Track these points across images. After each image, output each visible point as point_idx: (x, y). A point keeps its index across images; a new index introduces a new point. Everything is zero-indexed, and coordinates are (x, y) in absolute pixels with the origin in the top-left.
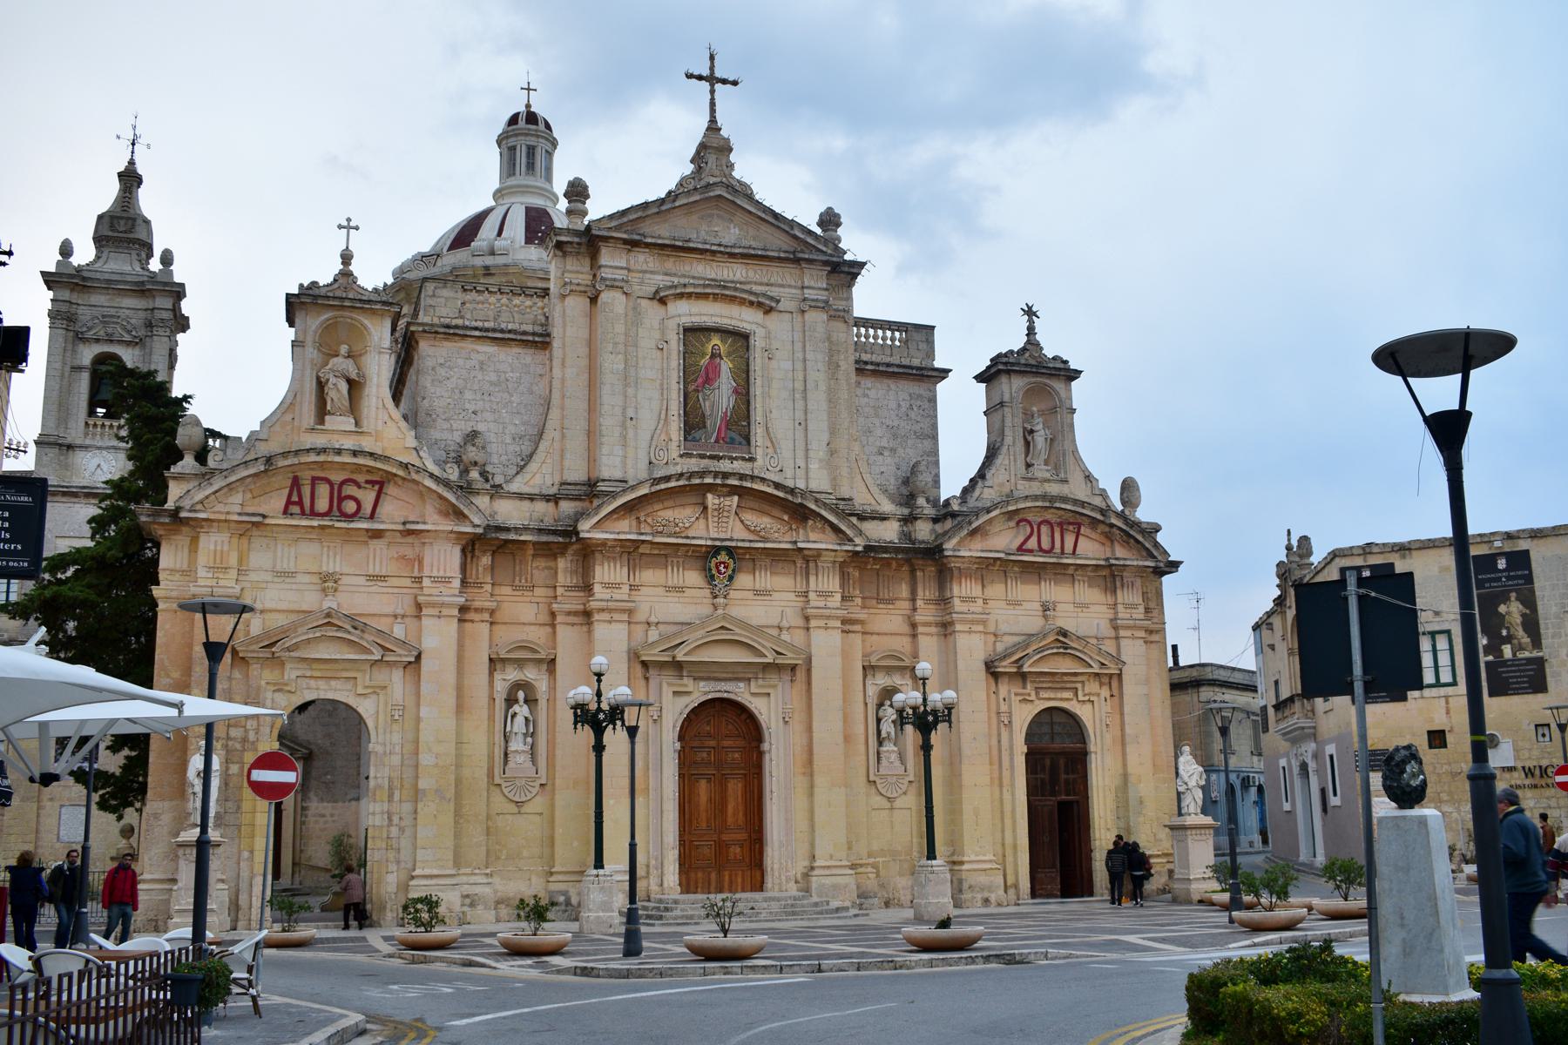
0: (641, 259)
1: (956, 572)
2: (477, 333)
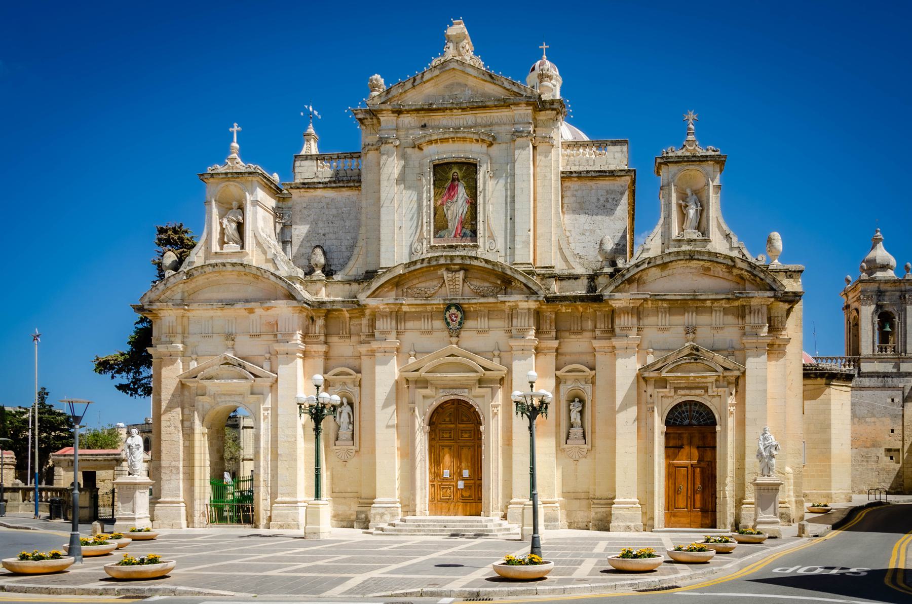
0: (407, 120)
1: (617, 311)
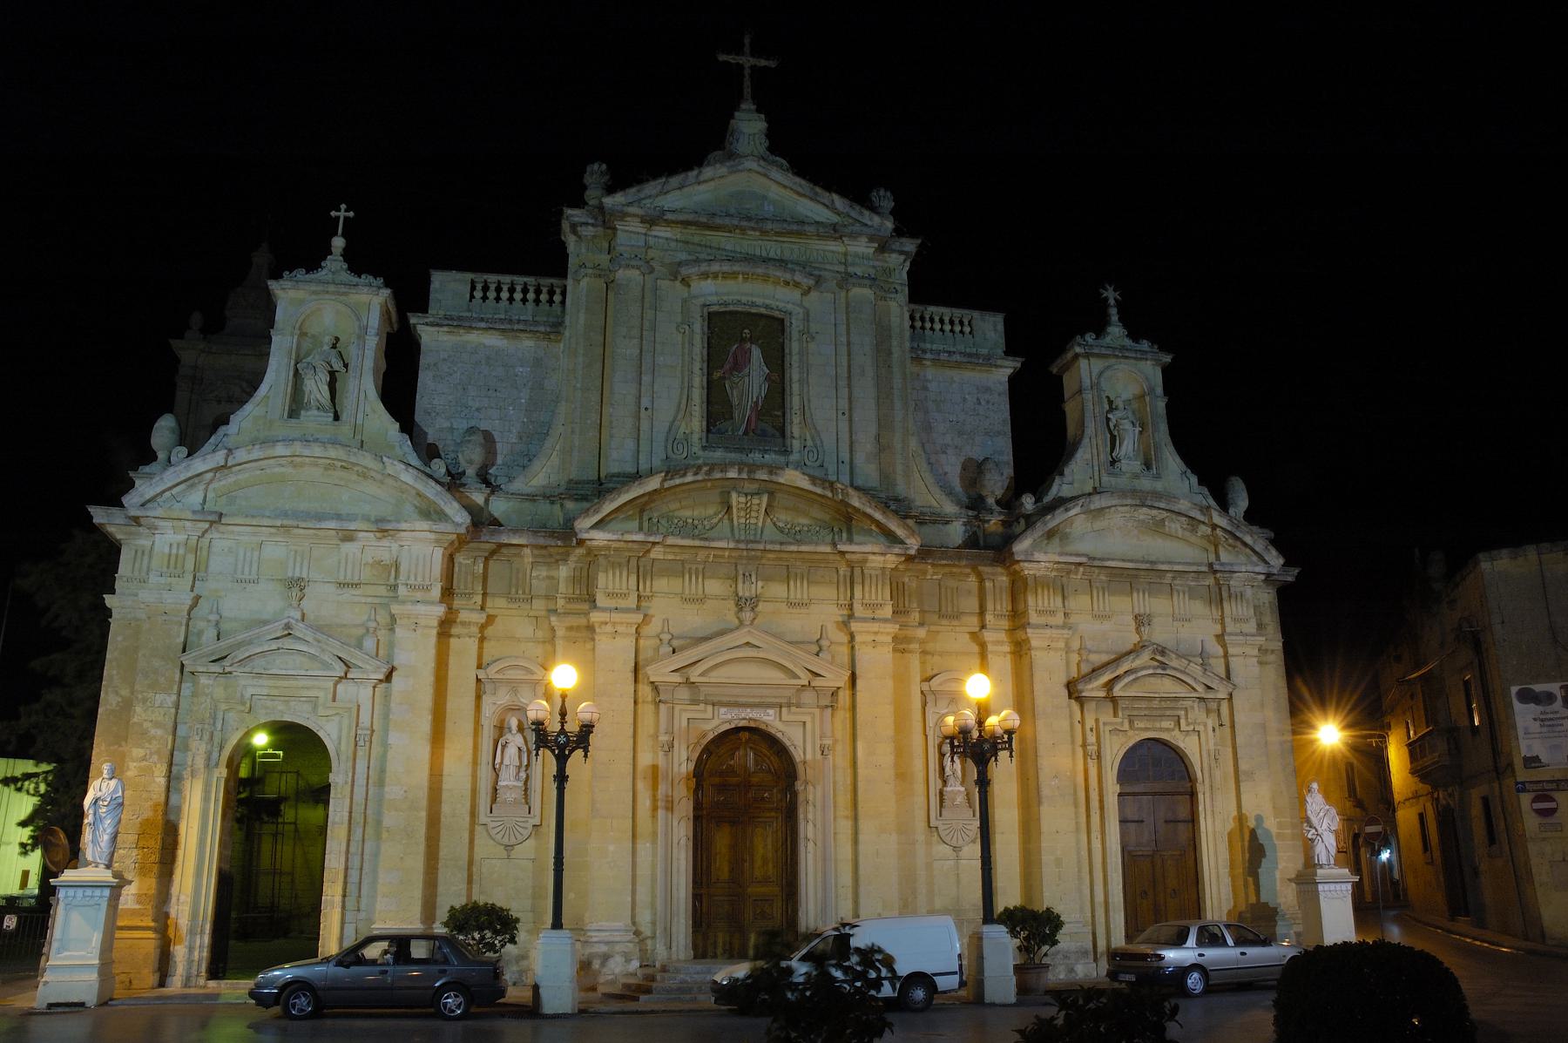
1: (1031, 581)
2: (483, 325)
